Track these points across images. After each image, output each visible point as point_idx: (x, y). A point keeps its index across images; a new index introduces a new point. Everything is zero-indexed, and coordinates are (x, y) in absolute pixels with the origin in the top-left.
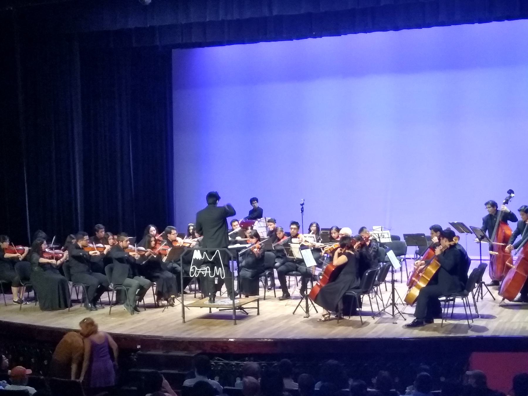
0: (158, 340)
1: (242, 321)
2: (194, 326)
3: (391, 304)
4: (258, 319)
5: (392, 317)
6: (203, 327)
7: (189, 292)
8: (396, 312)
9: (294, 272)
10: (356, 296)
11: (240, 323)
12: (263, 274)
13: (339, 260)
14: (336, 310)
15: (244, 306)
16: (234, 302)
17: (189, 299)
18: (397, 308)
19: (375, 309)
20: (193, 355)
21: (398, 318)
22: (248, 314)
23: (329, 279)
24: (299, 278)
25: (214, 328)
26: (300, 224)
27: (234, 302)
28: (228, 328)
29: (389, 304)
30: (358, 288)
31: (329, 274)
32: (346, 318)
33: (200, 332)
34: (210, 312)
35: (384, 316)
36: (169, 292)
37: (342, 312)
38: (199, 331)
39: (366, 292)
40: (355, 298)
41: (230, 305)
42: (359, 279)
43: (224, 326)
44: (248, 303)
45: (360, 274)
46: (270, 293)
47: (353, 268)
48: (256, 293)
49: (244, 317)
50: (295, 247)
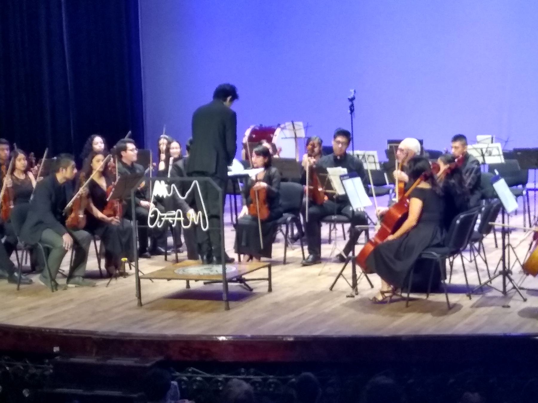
0: (90, 338)
1: (244, 302)
2: (155, 312)
3: (501, 273)
4: (269, 299)
5: (501, 295)
8: (509, 286)
9: (334, 217)
12: (280, 220)
15: (246, 277)
16: (224, 269)
17: (147, 266)
18: (511, 280)
19: (473, 280)
21: (511, 298)
22: (251, 290)
24: (347, 226)
27: (224, 269)
29: (497, 273)
30: (438, 245)
33: (164, 324)
34: (188, 286)
35: (489, 294)
39: (456, 251)
40: (437, 264)
41: (218, 275)
43: (207, 312)
45: (446, 222)
48: (267, 252)
49: (246, 294)
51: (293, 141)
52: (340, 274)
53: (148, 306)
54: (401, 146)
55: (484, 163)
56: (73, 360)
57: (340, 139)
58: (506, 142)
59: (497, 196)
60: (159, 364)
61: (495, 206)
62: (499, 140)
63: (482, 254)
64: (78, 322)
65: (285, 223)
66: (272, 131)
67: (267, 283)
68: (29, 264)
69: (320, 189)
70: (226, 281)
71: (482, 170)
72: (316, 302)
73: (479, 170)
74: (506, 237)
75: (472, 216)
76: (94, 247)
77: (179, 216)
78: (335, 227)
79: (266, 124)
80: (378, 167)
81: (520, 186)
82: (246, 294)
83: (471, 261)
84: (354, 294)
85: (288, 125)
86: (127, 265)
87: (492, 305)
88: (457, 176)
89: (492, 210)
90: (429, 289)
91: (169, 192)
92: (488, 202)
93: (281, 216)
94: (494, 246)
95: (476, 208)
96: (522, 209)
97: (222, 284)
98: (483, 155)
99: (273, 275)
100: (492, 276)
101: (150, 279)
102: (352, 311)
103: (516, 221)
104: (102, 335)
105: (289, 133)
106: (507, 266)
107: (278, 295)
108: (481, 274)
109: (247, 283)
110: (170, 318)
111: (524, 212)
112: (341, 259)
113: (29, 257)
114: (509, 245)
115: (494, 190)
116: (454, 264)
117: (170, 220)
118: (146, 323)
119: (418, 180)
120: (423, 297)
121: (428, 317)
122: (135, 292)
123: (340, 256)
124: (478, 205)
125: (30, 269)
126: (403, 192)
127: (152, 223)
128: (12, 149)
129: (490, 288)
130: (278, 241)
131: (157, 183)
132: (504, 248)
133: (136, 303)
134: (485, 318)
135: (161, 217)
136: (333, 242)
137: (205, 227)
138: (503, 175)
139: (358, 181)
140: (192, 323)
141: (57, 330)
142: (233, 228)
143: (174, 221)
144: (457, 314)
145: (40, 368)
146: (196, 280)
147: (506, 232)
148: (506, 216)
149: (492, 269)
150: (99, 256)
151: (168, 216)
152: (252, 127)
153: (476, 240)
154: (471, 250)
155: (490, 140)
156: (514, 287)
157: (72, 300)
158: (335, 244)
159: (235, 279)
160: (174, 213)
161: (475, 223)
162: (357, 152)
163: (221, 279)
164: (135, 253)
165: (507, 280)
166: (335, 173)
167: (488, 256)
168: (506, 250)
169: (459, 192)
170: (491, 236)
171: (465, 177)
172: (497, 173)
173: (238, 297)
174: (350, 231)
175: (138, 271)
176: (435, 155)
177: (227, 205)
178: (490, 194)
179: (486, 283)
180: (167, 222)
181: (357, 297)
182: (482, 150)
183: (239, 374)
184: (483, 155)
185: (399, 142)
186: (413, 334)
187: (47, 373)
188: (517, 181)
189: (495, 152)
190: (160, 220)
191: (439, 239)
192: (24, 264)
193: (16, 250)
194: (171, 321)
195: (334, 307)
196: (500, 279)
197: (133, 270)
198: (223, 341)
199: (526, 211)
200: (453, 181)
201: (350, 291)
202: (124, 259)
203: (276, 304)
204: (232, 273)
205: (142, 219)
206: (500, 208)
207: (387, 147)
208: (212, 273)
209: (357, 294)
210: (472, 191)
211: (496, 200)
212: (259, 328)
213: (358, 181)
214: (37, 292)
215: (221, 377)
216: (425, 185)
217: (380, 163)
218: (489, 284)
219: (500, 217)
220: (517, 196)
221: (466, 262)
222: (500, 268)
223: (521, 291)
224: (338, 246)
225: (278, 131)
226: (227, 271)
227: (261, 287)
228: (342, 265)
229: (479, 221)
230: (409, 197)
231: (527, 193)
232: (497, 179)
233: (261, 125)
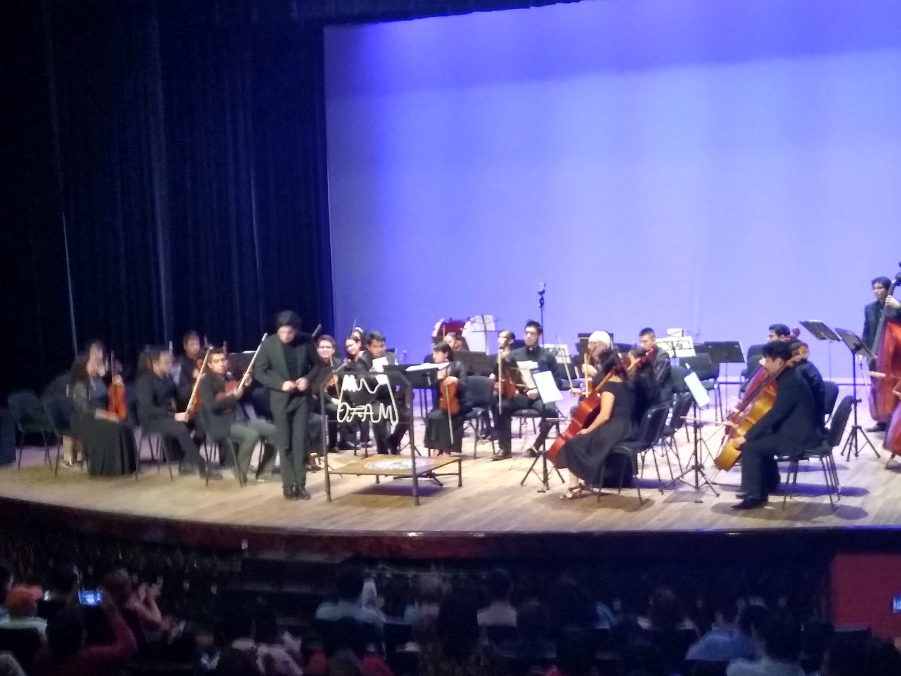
1: (431, 498)
3: (693, 468)
4: (460, 494)
5: (693, 490)
6: (362, 509)
8: (702, 481)
9: (524, 411)
10: (631, 455)
11: (424, 503)
15: (436, 472)
17: (335, 460)
18: (703, 475)
19: (665, 475)
20: (338, 561)
21: (703, 493)
24: (538, 420)
25: (379, 511)
29: (689, 468)
30: (630, 440)
33: (353, 520)
35: (682, 489)
38: (352, 516)
39: (648, 445)
40: (629, 458)
41: (408, 470)
42: (636, 426)
45: (637, 415)
48: (458, 447)
49: (436, 490)
51: (483, 334)
52: (531, 469)
53: (337, 502)
54: (591, 339)
55: (675, 357)
57: (532, 329)
58: (697, 335)
59: (688, 390)
60: (350, 561)
61: (687, 399)
62: (690, 333)
63: (674, 448)
65: (476, 417)
66: (462, 324)
67: (457, 477)
68: (217, 459)
69: (511, 382)
70: (416, 476)
71: (672, 364)
72: (506, 498)
73: (669, 363)
74: (698, 431)
75: (664, 410)
77: (368, 411)
78: (525, 421)
79: (456, 318)
80: (569, 361)
81: (711, 380)
82: (436, 490)
83: (663, 456)
84: (545, 489)
85: (478, 318)
86: (317, 460)
88: (648, 370)
89: (684, 404)
90: (621, 484)
92: (679, 397)
94: (686, 440)
95: (668, 402)
96: (713, 403)
98: (674, 349)
99: (463, 470)
100: (684, 471)
101: (340, 474)
102: (543, 506)
103: (706, 415)
105: (478, 327)
106: (699, 460)
108: (673, 469)
110: (360, 514)
111: (716, 406)
112: (532, 454)
114: (701, 439)
115: (685, 383)
116: (646, 458)
117: (359, 414)
118: (336, 519)
119: (609, 374)
120: (615, 492)
121: (620, 512)
123: (531, 450)
124: (670, 399)
126: (593, 385)
127: (341, 419)
128: (202, 343)
130: (468, 435)
131: (346, 377)
132: (696, 442)
133: (325, 498)
134: (678, 514)
135: (350, 411)
136: (524, 436)
138: (694, 368)
139: (549, 374)
140: (381, 519)
141: (245, 527)
142: (423, 422)
144: (649, 510)
146: (386, 476)
147: (697, 426)
148: (697, 410)
149: (684, 463)
152: (442, 320)
153: (667, 435)
154: (663, 444)
155: (680, 334)
156: (707, 483)
158: (526, 439)
160: (364, 407)
161: (667, 417)
162: (546, 346)
163: (411, 473)
164: (325, 448)
165: (699, 474)
166: (525, 366)
167: (680, 450)
168: (698, 444)
169: (650, 386)
170: (683, 429)
171: (655, 372)
172: (688, 366)
173: (428, 492)
174: (540, 425)
175: (327, 466)
176: (625, 348)
177: (417, 399)
178: (681, 388)
179: (678, 478)
180: (356, 416)
181: (548, 492)
182: (672, 343)
184: (674, 349)
185: (588, 335)
186: (606, 529)
188: (708, 374)
190: (350, 415)
191: (630, 433)
195: (524, 502)
196: (693, 473)
197: (323, 465)
198: (413, 537)
199: (718, 404)
200: (643, 375)
201: (541, 486)
202: (313, 454)
203: (466, 499)
204: (421, 467)
205: (332, 414)
206: (691, 402)
207: (578, 340)
208: (401, 468)
209: (548, 489)
210: (663, 385)
211: (687, 393)
213: (549, 374)
215: (411, 573)
216: (616, 379)
217: (570, 356)
219: (691, 411)
220: (708, 389)
221: (658, 457)
222: (693, 463)
223: (713, 486)
224: (528, 441)
225: (468, 325)
226: (417, 466)
227: (453, 481)
228: (534, 459)
229: (670, 415)
230: (601, 391)
231: (719, 388)
232: (688, 373)
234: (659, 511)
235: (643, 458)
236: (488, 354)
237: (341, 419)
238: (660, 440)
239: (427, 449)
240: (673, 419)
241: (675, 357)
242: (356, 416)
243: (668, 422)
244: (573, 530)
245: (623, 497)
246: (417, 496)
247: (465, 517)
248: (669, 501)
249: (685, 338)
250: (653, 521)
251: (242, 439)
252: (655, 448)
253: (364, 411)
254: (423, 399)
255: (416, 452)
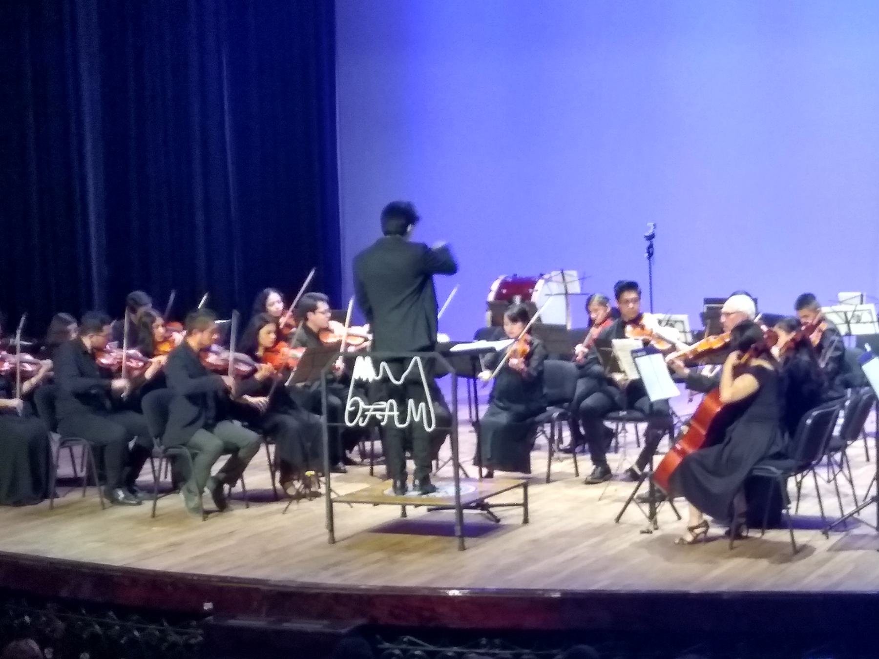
0: (257, 590)
3: (874, 499)
4: (525, 535)
6: (379, 555)
7: (358, 459)
9: (623, 413)
10: (780, 479)
11: (475, 546)
12: (541, 417)
13: (736, 388)
14: (722, 514)
15: (490, 501)
19: (832, 510)
22: (498, 521)
23: (708, 435)
24: (643, 426)
26: (643, 286)
28: (441, 558)
29: (869, 499)
30: (779, 456)
31: (709, 421)
32: (755, 534)
34: (404, 514)
35: (856, 531)
36: (310, 458)
37: (743, 520)
39: (806, 465)
41: (449, 498)
42: (787, 435)
44: (502, 489)
45: (790, 421)
46: (563, 466)
47: (772, 407)
48: (521, 464)
49: (489, 528)
50: (622, 347)
51: (563, 298)
55: (849, 334)
56: (233, 622)
57: (630, 295)
59: (868, 384)
60: (360, 631)
61: (865, 397)
62: (872, 299)
63: (846, 471)
64: (239, 567)
65: (550, 421)
67: (521, 510)
68: (169, 479)
70: (460, 507)
71: (846, 344)
76: (264, 456)
77: (391, 410)
78: (624, 428)
79: (523, 274)
83: (829, 481)
84: (651, 528)
85: (555, 274)
87: (859, 548)
89: (861, 404)
91: (378, 375)
93: (543, 410)
94: (865, 459)
97: (454, 511)
98: (848, 322)
99: (530, 500)
100: (860, 504)
101: (349, 503)
104: (275, 586)
105: (556, 287)
107: (538, 530)
108: (843, 501)
109: (491, 510)
112: (633, 476)
113: (170, 468)
115: (863, 376)
117: (378, 415)
118: (341, 568)
121: (764, 563)
122: (324, 521)
123: (631, 470)
124: (843, 397)
125: (171, 486)
127: (351, 421)
129: (858, 522)
130: (539, 448)
133: (326, 537)
135: (365, 410)
136: (621, 450)
137: (430, 425)
141: (209, 577)
142: (472, 429)
143: (383, 416)
145: (186, 633)
146: (417, 506)
149: (861, 492)
150: (274, 467)
151: (375, 410)
152: (502, 278)
153: (836, 450)
154: (829, 464)
155: (858, 300)
157: (231, 533)
158: (625, 454)
159: (474, 504)
160: (384, 405)
161: (834, 425)
163: (452, 503)
167: (855, 473)
172: (868, 348)
174: (647, 434)
175: (329, 490)
178: (858, 381)
179: (851, 515)
180: (373, 418)
181: (656, 534)
182: (845, 313)
183: (477, 646)
184: (848, 322)
185: (722, 301)
186: (741, 589)
187: (193, 641)
189: (866, 317)
190: (364, 416)
192: (162, 479)
193: (152, 458)
194: (377, 566)
197: (323, 490)
198: (455, 598)
201: (647, 524)
203: (535, 541)
207: (704, 308)
209: (656, 529)
211: (867, 388)
212: (510, 577)
214: (176, 518)
215: (451, 651)
217: (692, 332)
218: (855, 515)
221: (821, 482)
224: (628, 458)
226: (462, 493)
227: (513, 516)
228: (635, 484)
229: (841, 421)
233: (515, 275)
234: (821, 563)
235: (799, 485)
236: (569, 327)
237: (351, 421)
238: (825, 459)
239: (477, 469)
240: (845, 427)
241: (849, 334)
242: (373, 418)
243: (837, 431)
244: (694, 588)
245: (765, 542)
246: (462, 536)
247: (532, 569)
248: (836, 549)
249: (865, 306)
250: (812, 577)
251: (200, 449)
252: (818, 470)
253: (386, 411)
254: (473, 395)
255: (461, 472)
